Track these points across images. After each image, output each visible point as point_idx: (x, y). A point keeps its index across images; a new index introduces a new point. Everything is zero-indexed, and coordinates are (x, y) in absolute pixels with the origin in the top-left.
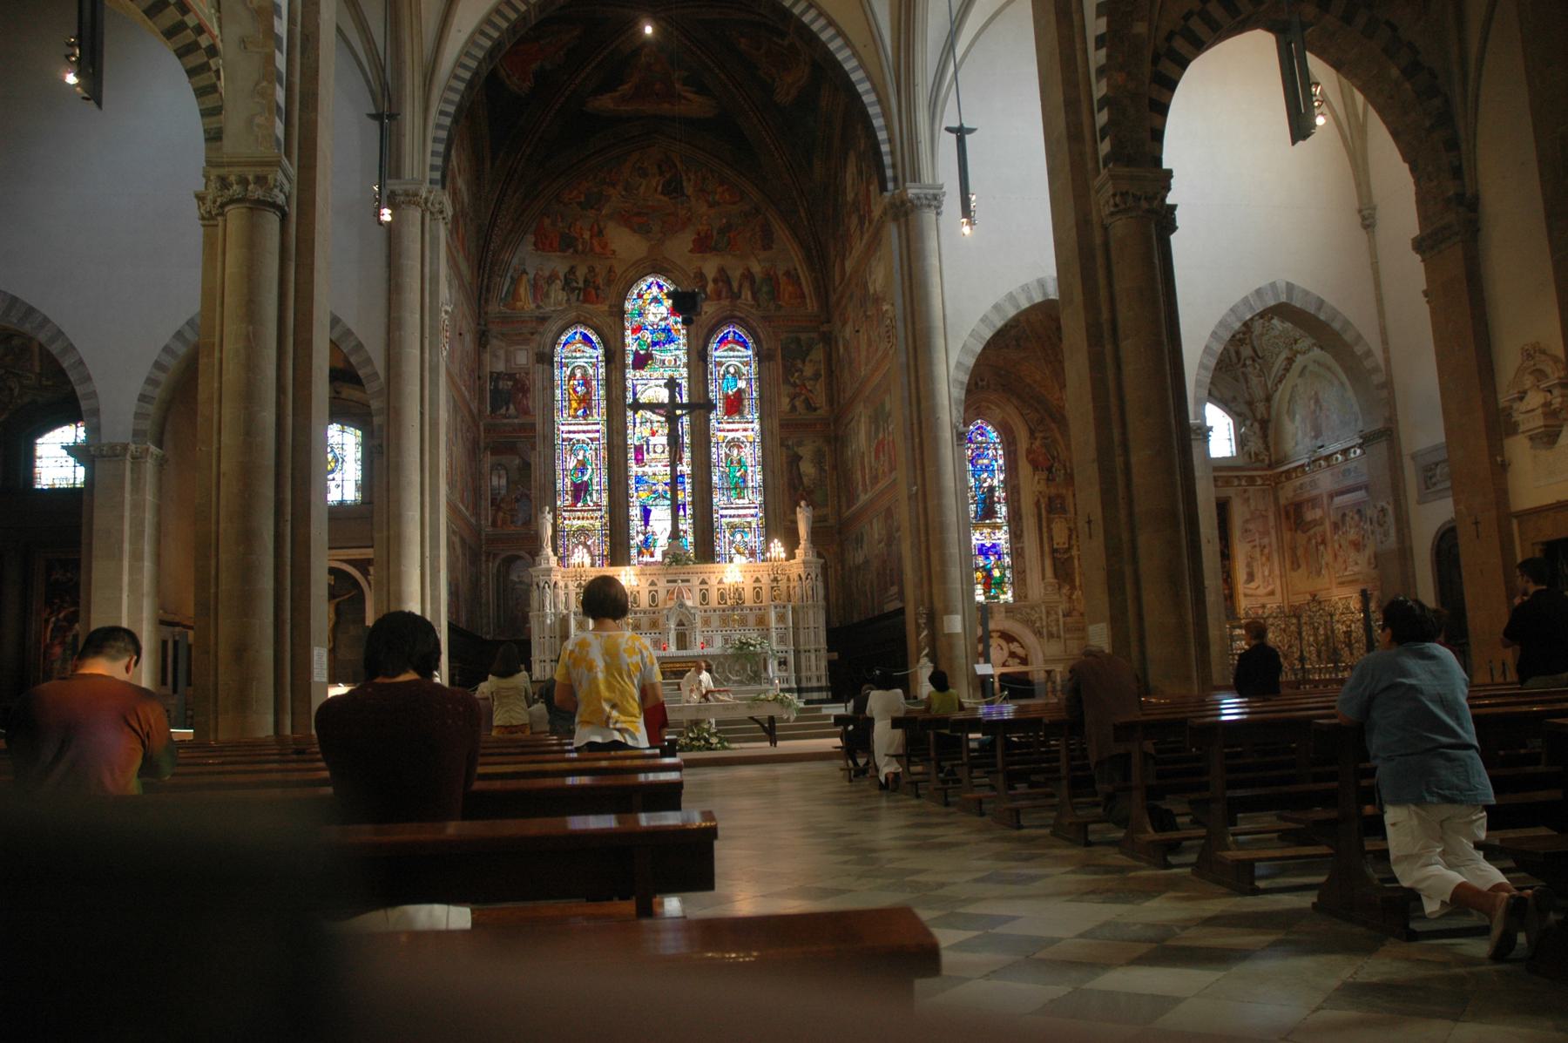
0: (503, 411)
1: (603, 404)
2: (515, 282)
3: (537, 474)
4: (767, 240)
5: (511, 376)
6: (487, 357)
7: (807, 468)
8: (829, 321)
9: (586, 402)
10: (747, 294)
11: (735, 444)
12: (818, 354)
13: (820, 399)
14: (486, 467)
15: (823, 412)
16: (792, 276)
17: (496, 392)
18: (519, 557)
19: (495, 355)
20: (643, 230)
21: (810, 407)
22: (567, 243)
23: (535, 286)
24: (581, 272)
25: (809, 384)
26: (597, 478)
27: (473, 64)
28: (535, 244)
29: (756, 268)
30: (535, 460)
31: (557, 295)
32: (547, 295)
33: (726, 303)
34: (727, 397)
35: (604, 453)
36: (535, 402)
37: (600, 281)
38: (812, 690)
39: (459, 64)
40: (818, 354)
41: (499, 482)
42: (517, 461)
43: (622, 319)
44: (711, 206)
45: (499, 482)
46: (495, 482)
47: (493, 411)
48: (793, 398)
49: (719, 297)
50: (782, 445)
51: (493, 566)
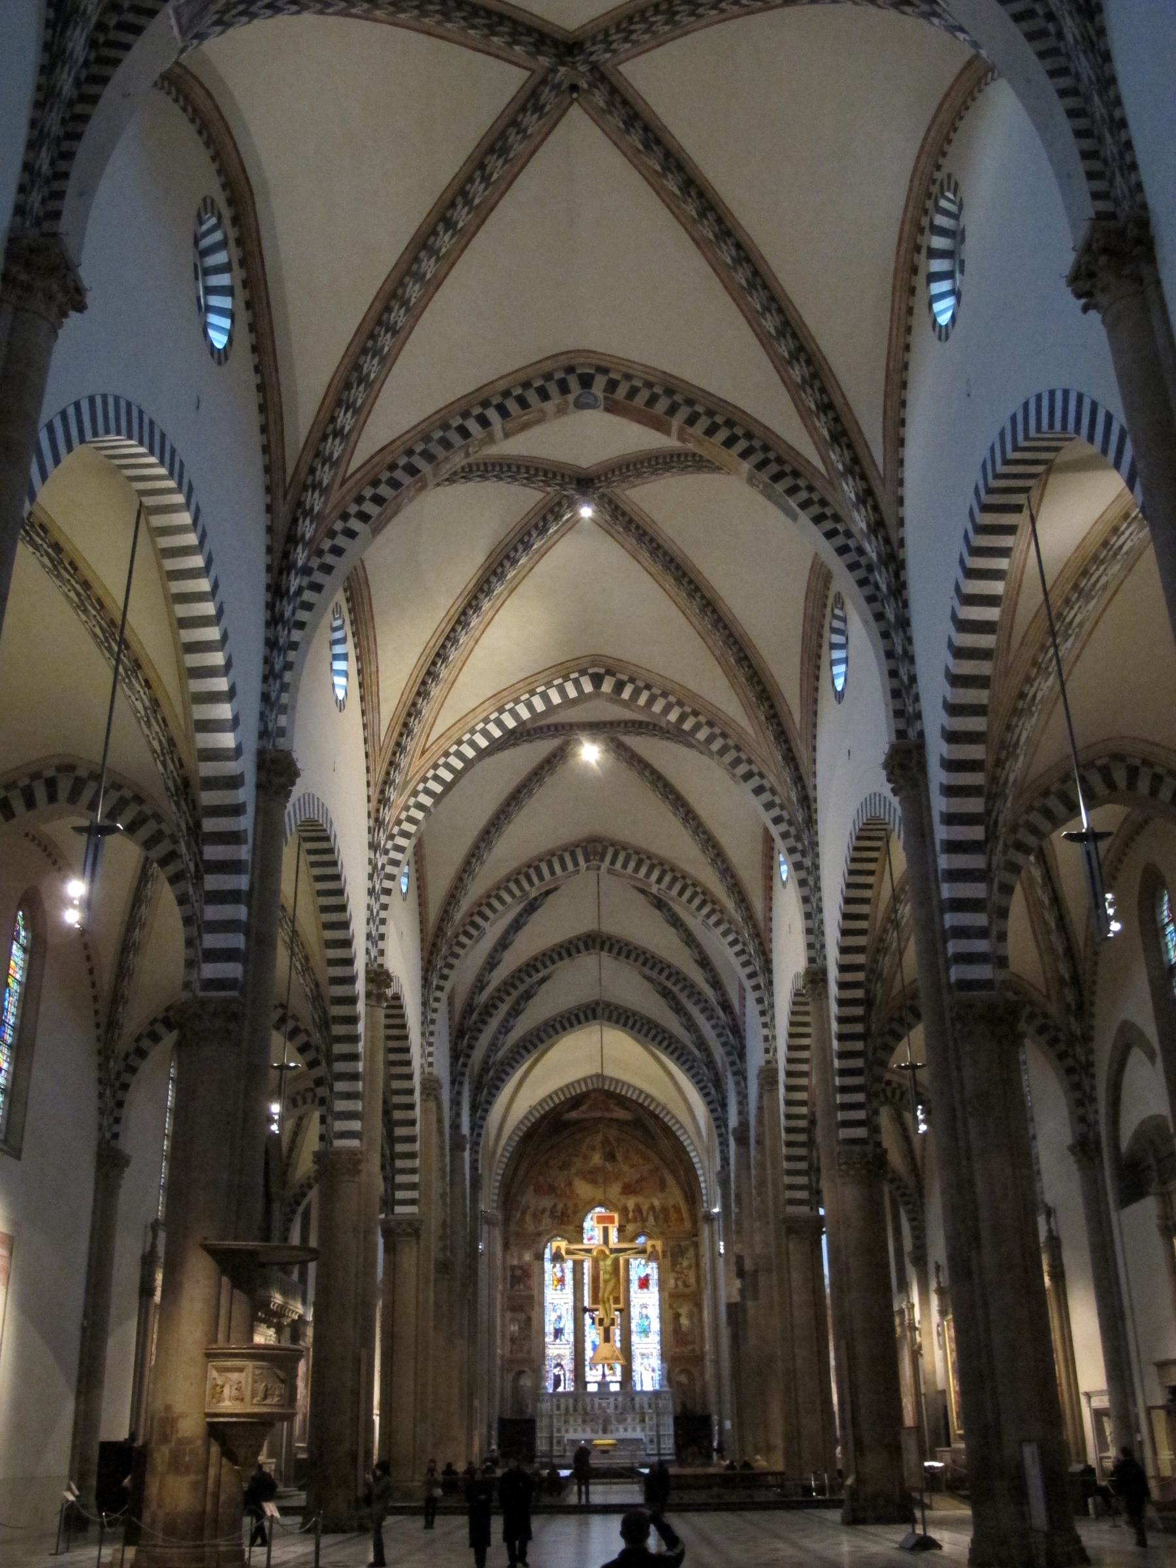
0: (517, 1287)
1: (571, 1282)
2: (523, 1213)
3: (535, 1323)
4: (663, 1186)
5: (521, 1268)
6: (508, 1257)
7: (684, 1321)
8: (696, 1235)
9: (561, 1281)
10: (651, 1219)
11: (644, 1306)
12: (691, 1253)
13: (692, 1280)
14: (507, 1319)
15: (694, 1287)
16: (677, 1209)
17: (513, 1276)
18: (523, 1372)
19: (512, 1256)
20: (594, 1182)
21: (686, 1285)
22: (552, 1190)
23: (534, 1216)
24: (560, 1206)
25: (686, 1271)
26: (568, 1325)
27: (511, 1149)
28: (535, 1191)
29: (657, 1203)
30: (534, 1315)
31: (546, 1221)
32: (540, 1221)
33: (639, 1224)
34: (640, 1279)
35: (571, 1311)
36: (534, 1282)
37: (570, 1212)
38: (665, 1455)
39: (504, 1149)
40: (691, 1253)
41: (514, 1328)
42: (523, 1316)
43: (582, 1233)
44: (632, 1166)
45: (514, 1328)
46: (512, 1328)
47: (512, 1286)
48: (676, 1279)
49: (635, 1220)
50: (671, 1307)
51: (510, 1377)
